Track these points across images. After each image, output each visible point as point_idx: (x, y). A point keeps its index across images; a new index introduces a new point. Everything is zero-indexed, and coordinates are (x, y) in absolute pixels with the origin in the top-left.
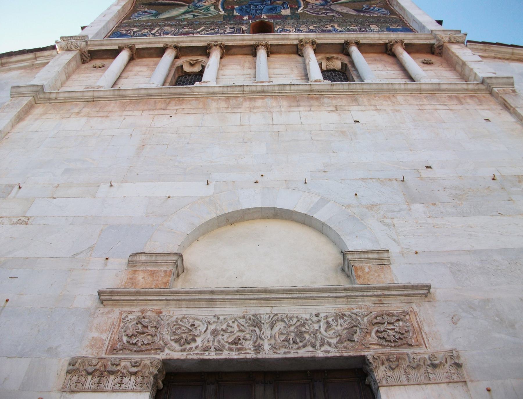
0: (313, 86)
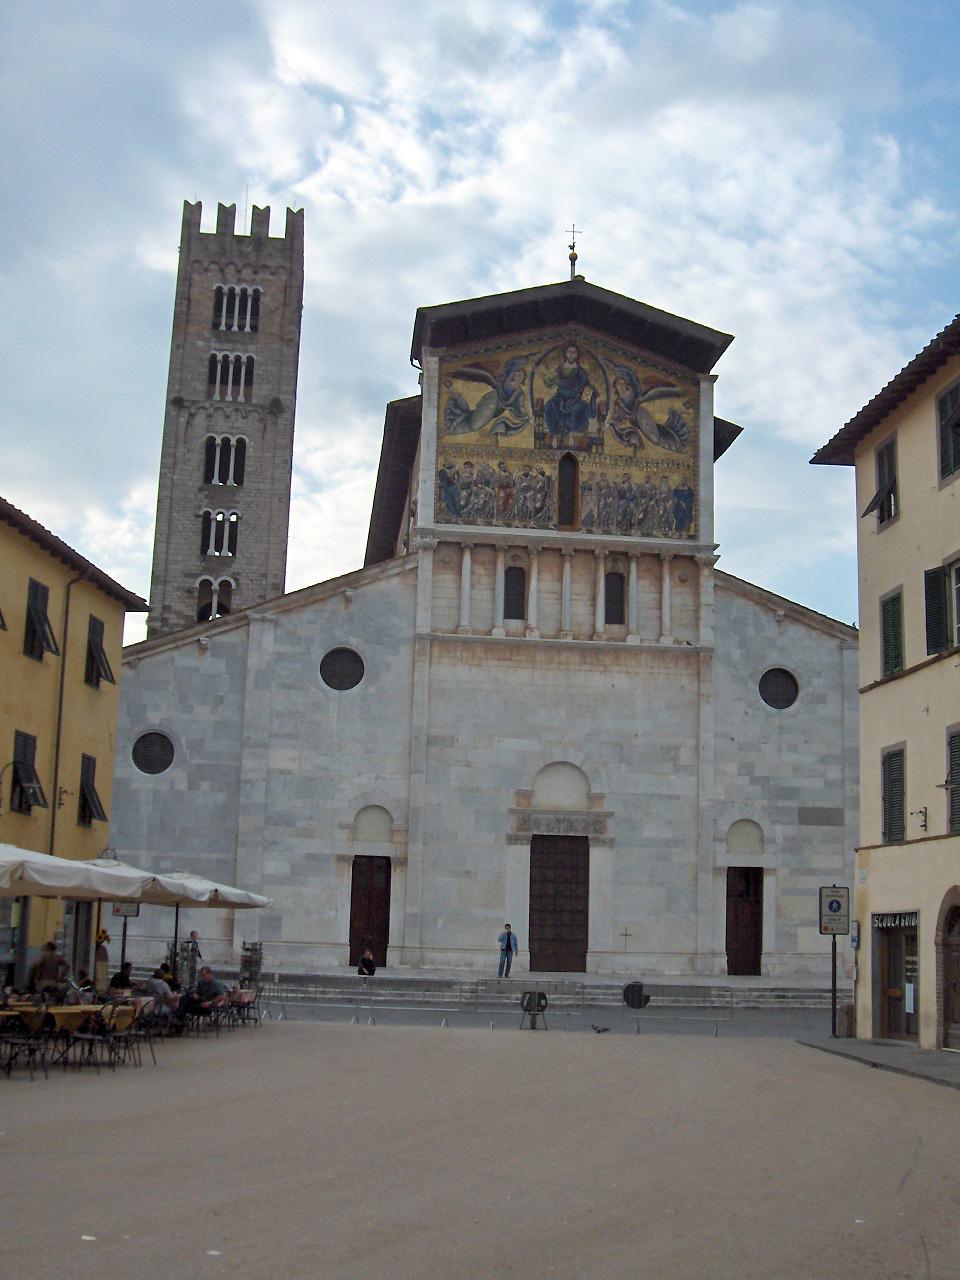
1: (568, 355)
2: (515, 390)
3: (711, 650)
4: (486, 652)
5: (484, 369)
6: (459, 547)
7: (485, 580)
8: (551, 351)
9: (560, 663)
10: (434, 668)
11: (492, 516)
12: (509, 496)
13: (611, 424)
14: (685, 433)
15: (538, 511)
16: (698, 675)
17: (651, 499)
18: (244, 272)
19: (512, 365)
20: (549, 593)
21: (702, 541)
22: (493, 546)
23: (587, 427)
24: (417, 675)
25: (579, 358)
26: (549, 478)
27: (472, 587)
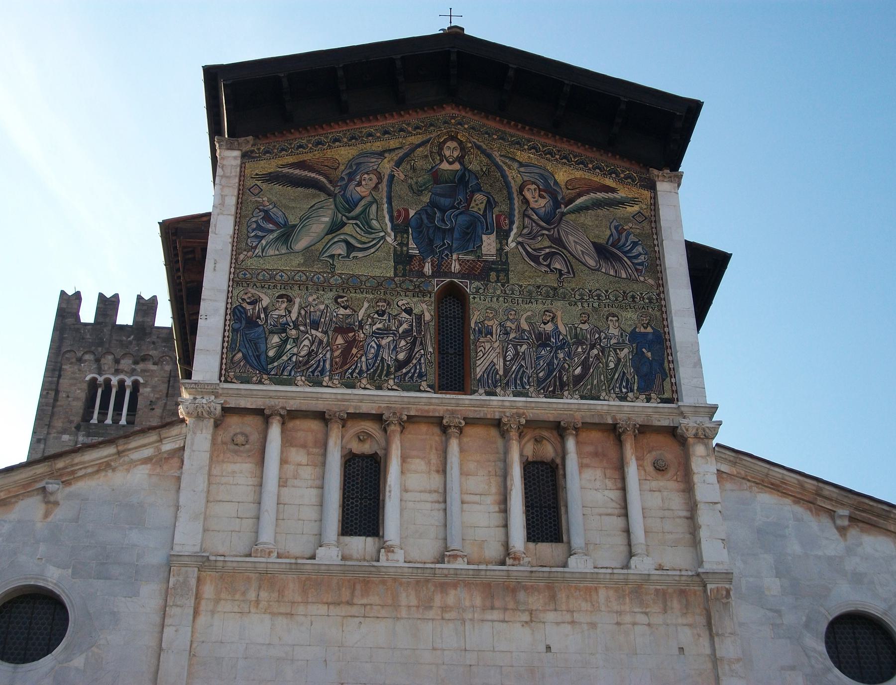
0: (510, 573)
1: (447, 153)
2: (362, 198)
3: (728, 576)
4: (304, 591)
5: (311, 169)
6: (263, 415)
7: (308, 473)
8: (419, 146)
9: (445, 608)
10: (202, 620)
11: (322, 372)
12: (350, 344)
13: (519, 243)
14: (640, 254)
15: (400, 365)
16: (709, 625)
17: (592, 348)
18: (122, 362)
19: (358, 164)
20: (421, 492)
21: (688, 399)
22: (321, 416)
23: (481, 246)
24: (168, 632)
25: (463, 157)
26: (420, 317)
27: (283, 483)
